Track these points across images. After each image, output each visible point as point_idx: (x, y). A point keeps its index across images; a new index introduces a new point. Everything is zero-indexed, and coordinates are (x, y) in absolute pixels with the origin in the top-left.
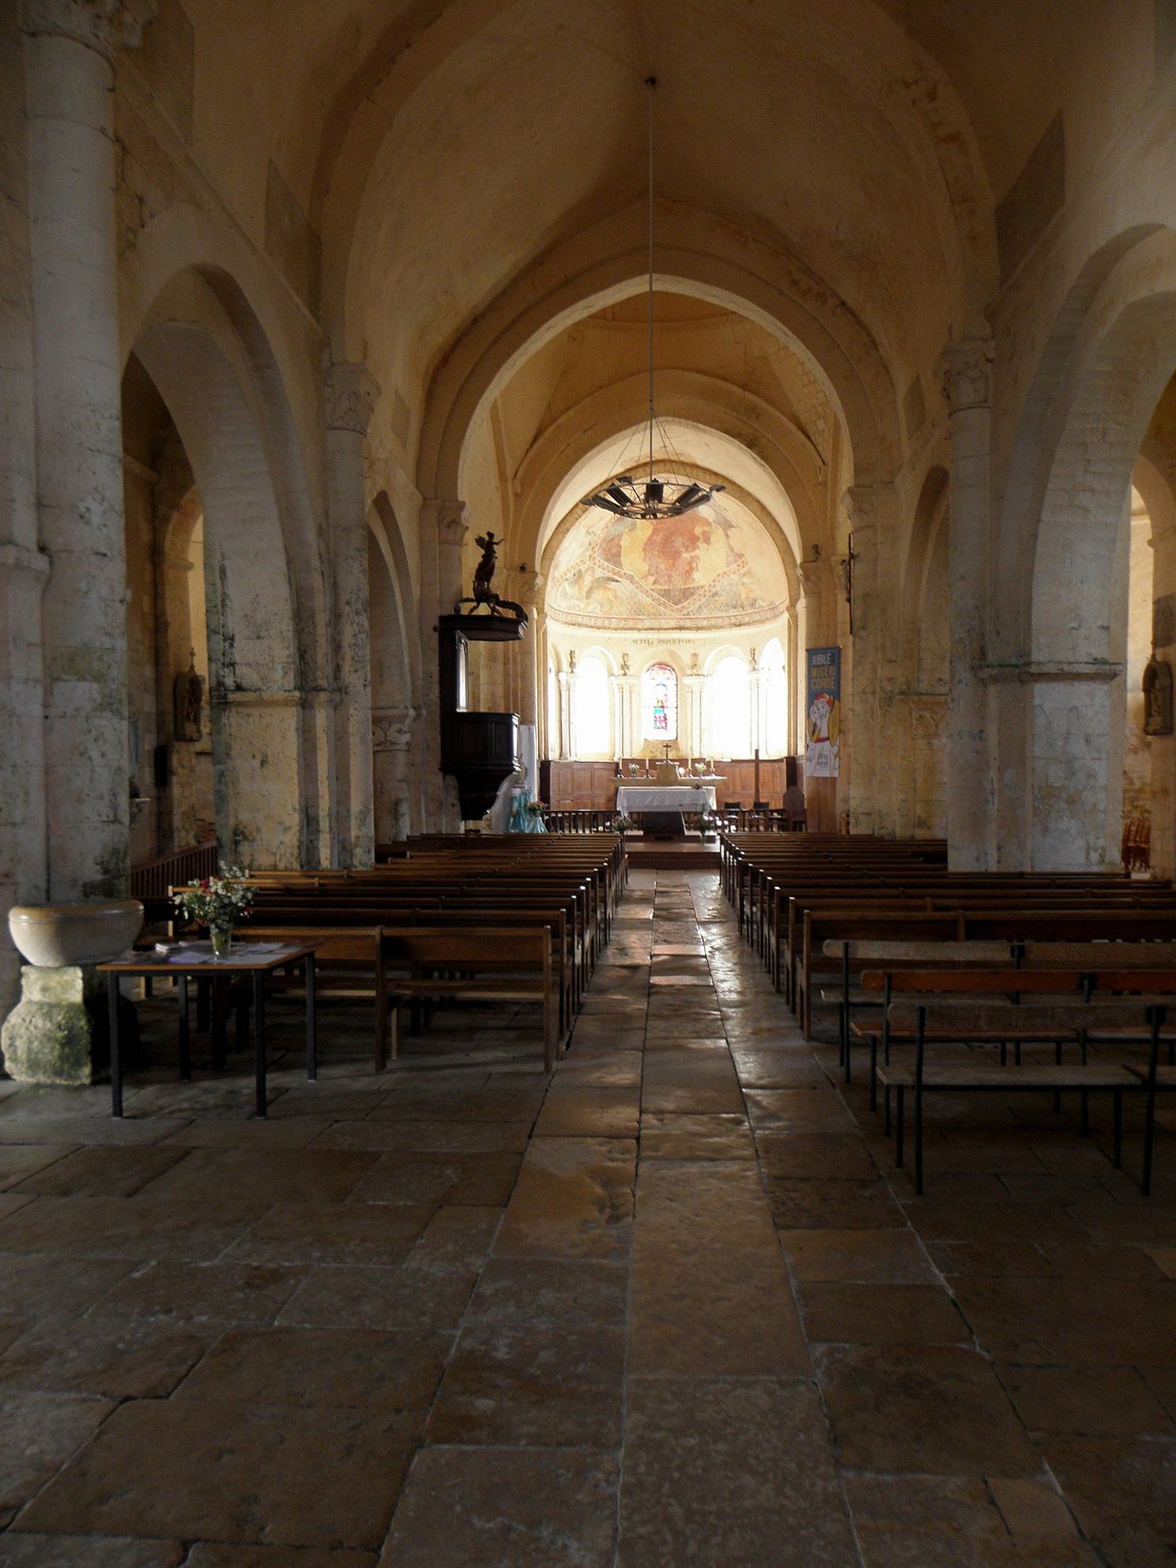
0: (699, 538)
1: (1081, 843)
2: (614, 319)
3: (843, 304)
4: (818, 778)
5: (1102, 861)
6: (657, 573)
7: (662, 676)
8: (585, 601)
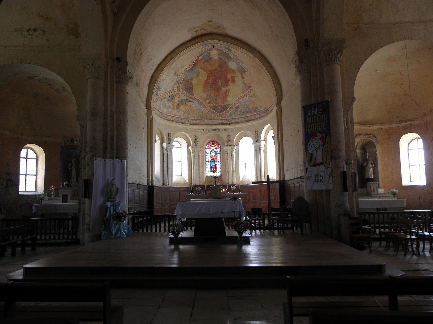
0: (229, 80)
4: (316, 190)
6: (210, 98)
7: (213, 147)
8: (176, 110)
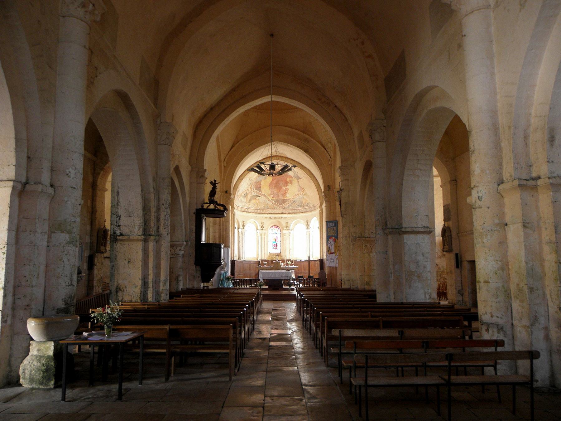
1: (422, 291)
2: (259, 109)
3: (336, 106)
4: (331, 267)
5: (430, 298)
7: (276, 230)
